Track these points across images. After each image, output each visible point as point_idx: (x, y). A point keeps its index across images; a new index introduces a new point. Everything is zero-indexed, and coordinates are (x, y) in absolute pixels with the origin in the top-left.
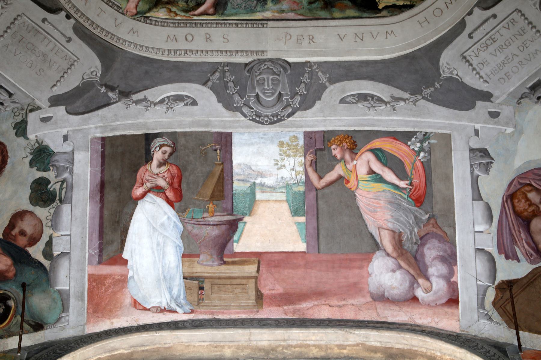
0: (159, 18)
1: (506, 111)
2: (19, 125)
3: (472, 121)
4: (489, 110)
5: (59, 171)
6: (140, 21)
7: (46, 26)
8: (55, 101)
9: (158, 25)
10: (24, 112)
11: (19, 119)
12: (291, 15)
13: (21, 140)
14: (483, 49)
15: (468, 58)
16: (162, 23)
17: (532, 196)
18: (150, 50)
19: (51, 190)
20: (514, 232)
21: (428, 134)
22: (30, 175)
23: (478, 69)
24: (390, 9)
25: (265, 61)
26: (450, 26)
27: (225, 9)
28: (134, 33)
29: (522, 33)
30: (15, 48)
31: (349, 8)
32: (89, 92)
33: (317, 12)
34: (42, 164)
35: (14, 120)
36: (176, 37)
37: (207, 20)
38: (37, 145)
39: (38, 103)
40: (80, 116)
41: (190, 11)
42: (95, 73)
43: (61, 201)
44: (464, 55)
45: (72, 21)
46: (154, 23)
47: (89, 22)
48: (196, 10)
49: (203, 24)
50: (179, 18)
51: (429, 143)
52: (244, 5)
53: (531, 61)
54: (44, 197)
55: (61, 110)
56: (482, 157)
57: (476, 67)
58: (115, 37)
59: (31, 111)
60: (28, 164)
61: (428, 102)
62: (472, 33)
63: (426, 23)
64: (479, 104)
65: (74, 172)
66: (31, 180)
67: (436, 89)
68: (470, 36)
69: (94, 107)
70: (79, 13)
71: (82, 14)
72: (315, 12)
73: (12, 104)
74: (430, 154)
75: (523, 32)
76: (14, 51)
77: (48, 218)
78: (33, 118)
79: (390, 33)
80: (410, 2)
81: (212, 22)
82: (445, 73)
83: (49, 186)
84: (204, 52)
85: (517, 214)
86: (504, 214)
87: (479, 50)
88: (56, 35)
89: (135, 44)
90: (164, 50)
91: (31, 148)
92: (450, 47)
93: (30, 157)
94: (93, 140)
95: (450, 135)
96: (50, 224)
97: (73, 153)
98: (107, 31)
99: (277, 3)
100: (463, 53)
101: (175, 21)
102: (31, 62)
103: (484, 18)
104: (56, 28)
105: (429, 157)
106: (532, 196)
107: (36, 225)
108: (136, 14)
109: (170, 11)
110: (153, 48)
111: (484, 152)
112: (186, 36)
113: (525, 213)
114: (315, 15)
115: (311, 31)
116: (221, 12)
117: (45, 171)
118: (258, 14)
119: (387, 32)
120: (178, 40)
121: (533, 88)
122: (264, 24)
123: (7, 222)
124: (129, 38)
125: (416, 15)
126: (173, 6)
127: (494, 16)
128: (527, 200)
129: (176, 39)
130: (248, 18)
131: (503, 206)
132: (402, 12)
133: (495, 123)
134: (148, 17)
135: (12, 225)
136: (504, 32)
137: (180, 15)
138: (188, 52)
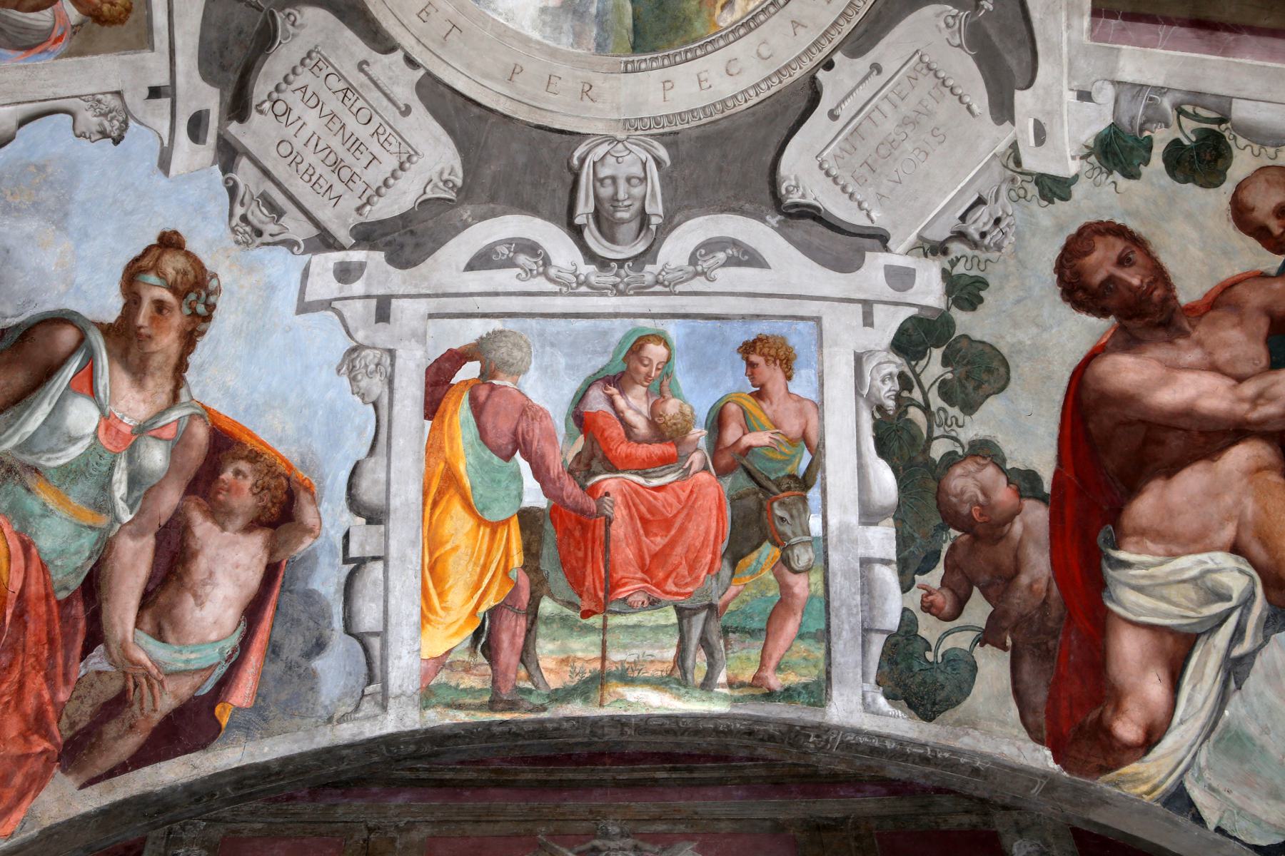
2: (1046, 191)
5: (1155, 117)
7: (846, 112)
8: (1003, 110)
10: (1019, 178)
11: (1033, 190)
13: (1077, 191)
19: (1194, 139)
22: (1155, 180)
30: (885, 181)
32: (988, 37)
34: (1135, 153)
35: (1035, 200)
38: (1093, 159)
39: (1002, 146)
40: (1041, 60)
42: (950, 21)
43: (1222, 120)
45: (838, 57)
54: (1208, 157)
55: (1023, 100)
59: (1018, 163)
60: (1132, 182)
65: (1160, 84)
66: (1167, 179)
69: (1024, 27)
71: (824, 35)
73: (1000, 201)
76: (891, 184)
77: (1256, 152)
78: (1033, 162)
83: (1186, 142)
88: (864, 93)
91: (1097, 171)
93: (1117, 176)
94: (1095, 35)
96: (1271, 151)
97: (1119, 83)
102: (916, 152)
104: (850, 94)
107: (1267, 181)
117: (1151, 148)
123: (1252, 242)
135: (1260, 233)
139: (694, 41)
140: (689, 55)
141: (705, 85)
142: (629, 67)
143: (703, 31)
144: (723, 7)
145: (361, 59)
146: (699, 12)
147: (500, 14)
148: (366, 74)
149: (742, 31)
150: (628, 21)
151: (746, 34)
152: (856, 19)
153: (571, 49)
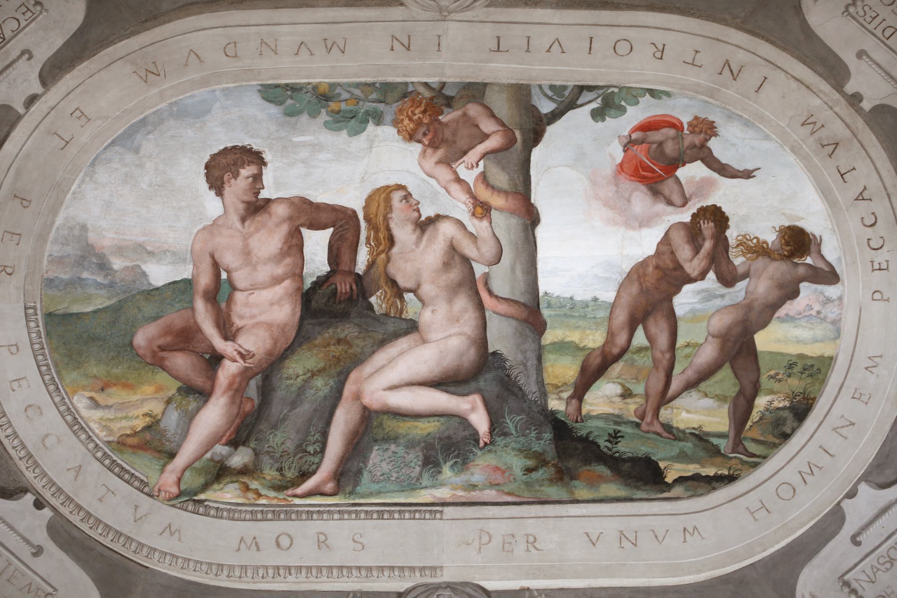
0: (223, 503)
6: (186, 510)
9: (221, 518)
12: (490, 495)
14: (883, 568)
15: (854, 585)
16: (231, 513)
18: (204, 567)
24: (690, 483)
25: (438, 587)
26: (812, 519)
27: (356, 484)
28: (172, 534)
31: (607, 481)
33: (543, 488)
36: (258, 540)
37: (320, 505)
41: (287, 488)
44: (846, 578)
45: (47, 513)
46: (212, 512)
47: (81, 513)
48: (299, 485)
49: (312, 512)
50: (263, 501)
52: (395, 475)
58: (134, 544)
63: (763, 512)
68: (855, 541)
70: (62, 497)
72: (537, 488)
79: (691, 530)
80: (730, 469)
81: (332, 509)
84: (314, 572)
87: (875, 570)
88: (13, 541)
89: (173, 556)
90: (231, 567)
92: (816, 561)
98: (117, 532)
99: (463, 470)
100: (843, 575)
101: (256, 509)
103: (882, 504)
104: (12, 528)
108: (178, 496)
109: (247, 488)
110: (210, 564)
112: (278, 537)
114: (539, 495)
115: (531, 526)
116: (348, 489)
118: (423, 492)
119: (685, 529)
120: (261, 546)
122: (436, 512)
124: (162, 544)
125: (742, 496)
126: (254, 478)
129: (256, 544)
130: (403, 500)
132: (714, 489)
134: (201, 502)
137: (267, 497)
138: (282, 572)
139: (58, 373)
140: (44, 368)
141: (15, 385)
142: (31, 311)
143: (67, 381)
144: (91, 398)
145: (34, 53)
146: (87, 376)
147: (79, 186)
148: (19, 58)
149: (69, 418)
150: (75, 309)
151: (66, 422)
152: (84, 527)
153: (47, 254)
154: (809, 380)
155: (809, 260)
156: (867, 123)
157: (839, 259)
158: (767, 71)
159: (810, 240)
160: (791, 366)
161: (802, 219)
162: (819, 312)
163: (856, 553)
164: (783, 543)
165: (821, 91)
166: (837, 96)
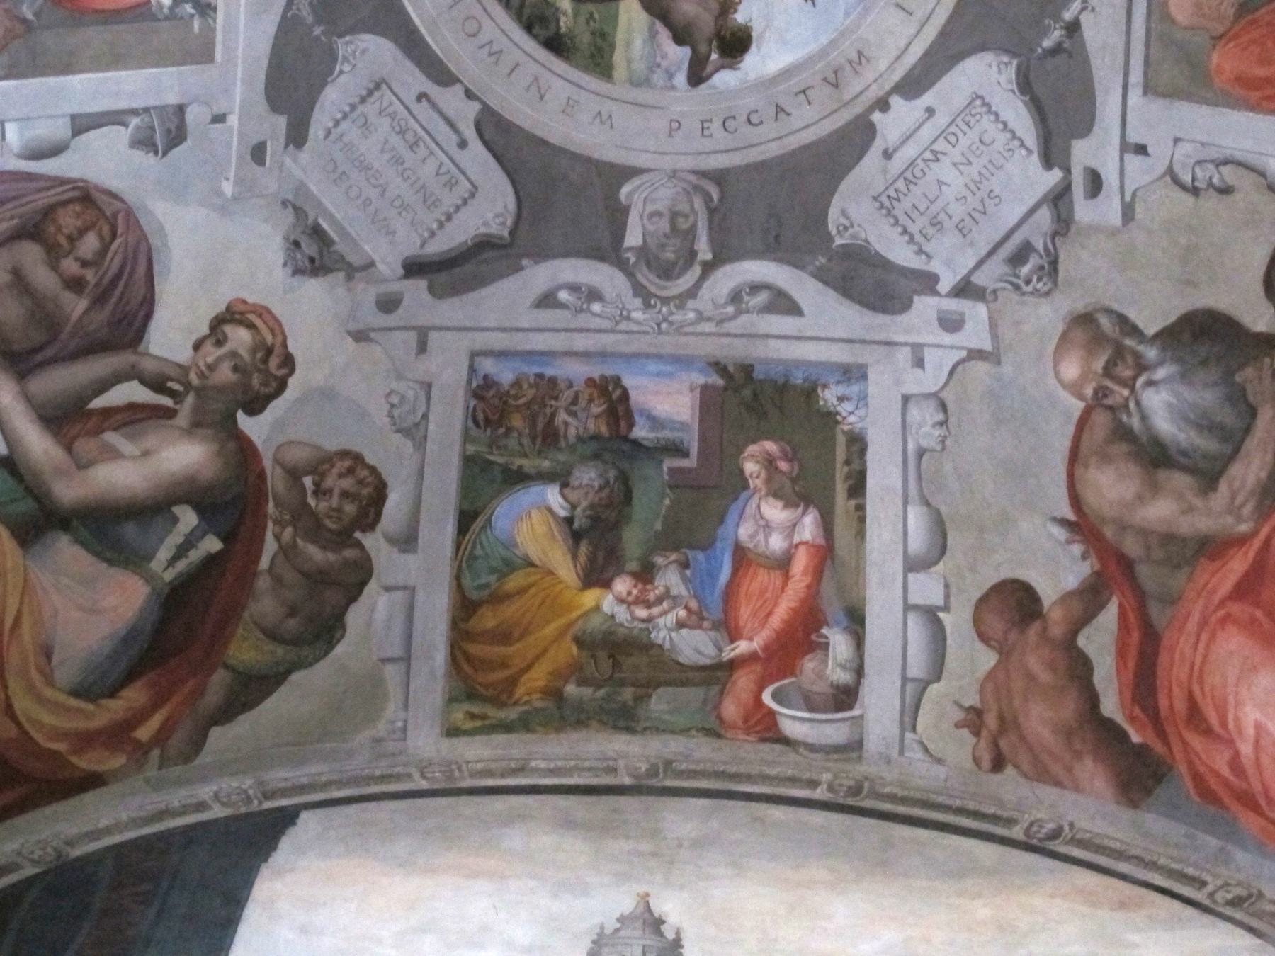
1: (268, 180)
3: (242, 107)
4: (269, 144)
14: (395, 124)
15: (377, 94)
17: (90, 243)
20: (10, 205)
21: (212, 13)
23: (354, 115)
29: (429, 203)
44: (384, 86)
51: (192, 16)
53: (373, 223)
56: (165, 132)
57: (358, 112)
61: (281, 10)
62: (429, 100)
64: (281, 122)
67: (311, 28)
68: (422, 97)
74: (167, 18)
75: (430, 202)
82: (344, 46)
85: (49, 212)
86: (48, 184)
87: (393, 116)
92: (399, 54)
95: (210, 58)
100: (387, 84)
105: (160, 16)
106: (90, 243)
111: (177, 136)
113: (52, 229)
121: (317, 232)
127: (463, 144)
128: (82, 232)
131: (62, 181)
133: (240, 157)
136: (431, 165)
154: (587, 53)
155: (714, 56)
156: (858, 117)
157: (715, 87)
158: (920, 15)
159: (735, 57)
160: (603, 35)
161: (759, 50)
162: (659, 66)
163: (410, 98)
164: (417, 22)
165: (894, 70)
166: (888, 87)
